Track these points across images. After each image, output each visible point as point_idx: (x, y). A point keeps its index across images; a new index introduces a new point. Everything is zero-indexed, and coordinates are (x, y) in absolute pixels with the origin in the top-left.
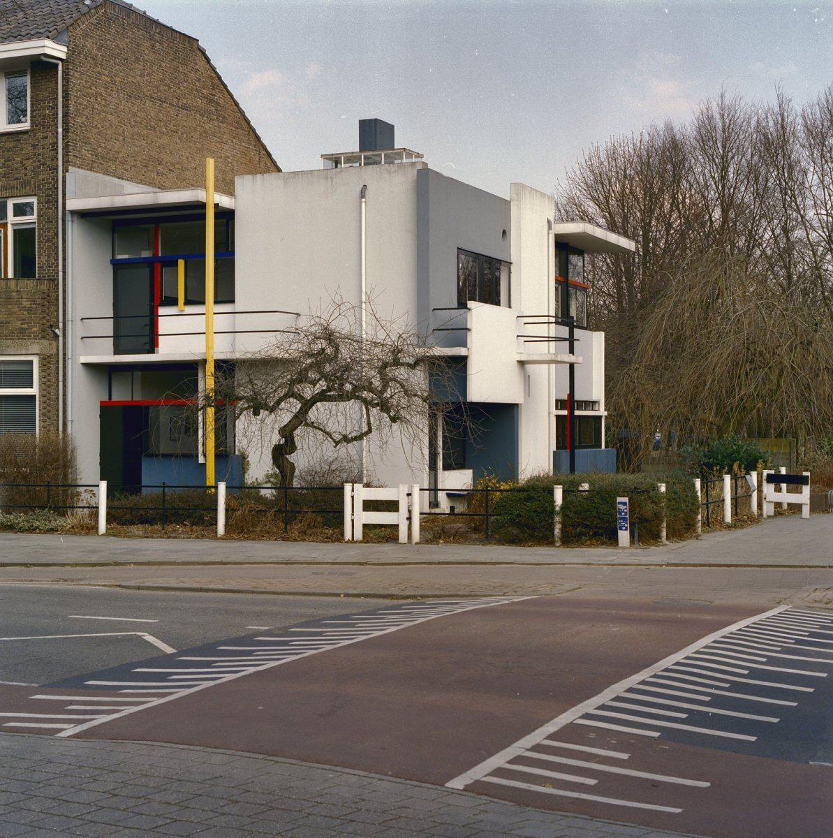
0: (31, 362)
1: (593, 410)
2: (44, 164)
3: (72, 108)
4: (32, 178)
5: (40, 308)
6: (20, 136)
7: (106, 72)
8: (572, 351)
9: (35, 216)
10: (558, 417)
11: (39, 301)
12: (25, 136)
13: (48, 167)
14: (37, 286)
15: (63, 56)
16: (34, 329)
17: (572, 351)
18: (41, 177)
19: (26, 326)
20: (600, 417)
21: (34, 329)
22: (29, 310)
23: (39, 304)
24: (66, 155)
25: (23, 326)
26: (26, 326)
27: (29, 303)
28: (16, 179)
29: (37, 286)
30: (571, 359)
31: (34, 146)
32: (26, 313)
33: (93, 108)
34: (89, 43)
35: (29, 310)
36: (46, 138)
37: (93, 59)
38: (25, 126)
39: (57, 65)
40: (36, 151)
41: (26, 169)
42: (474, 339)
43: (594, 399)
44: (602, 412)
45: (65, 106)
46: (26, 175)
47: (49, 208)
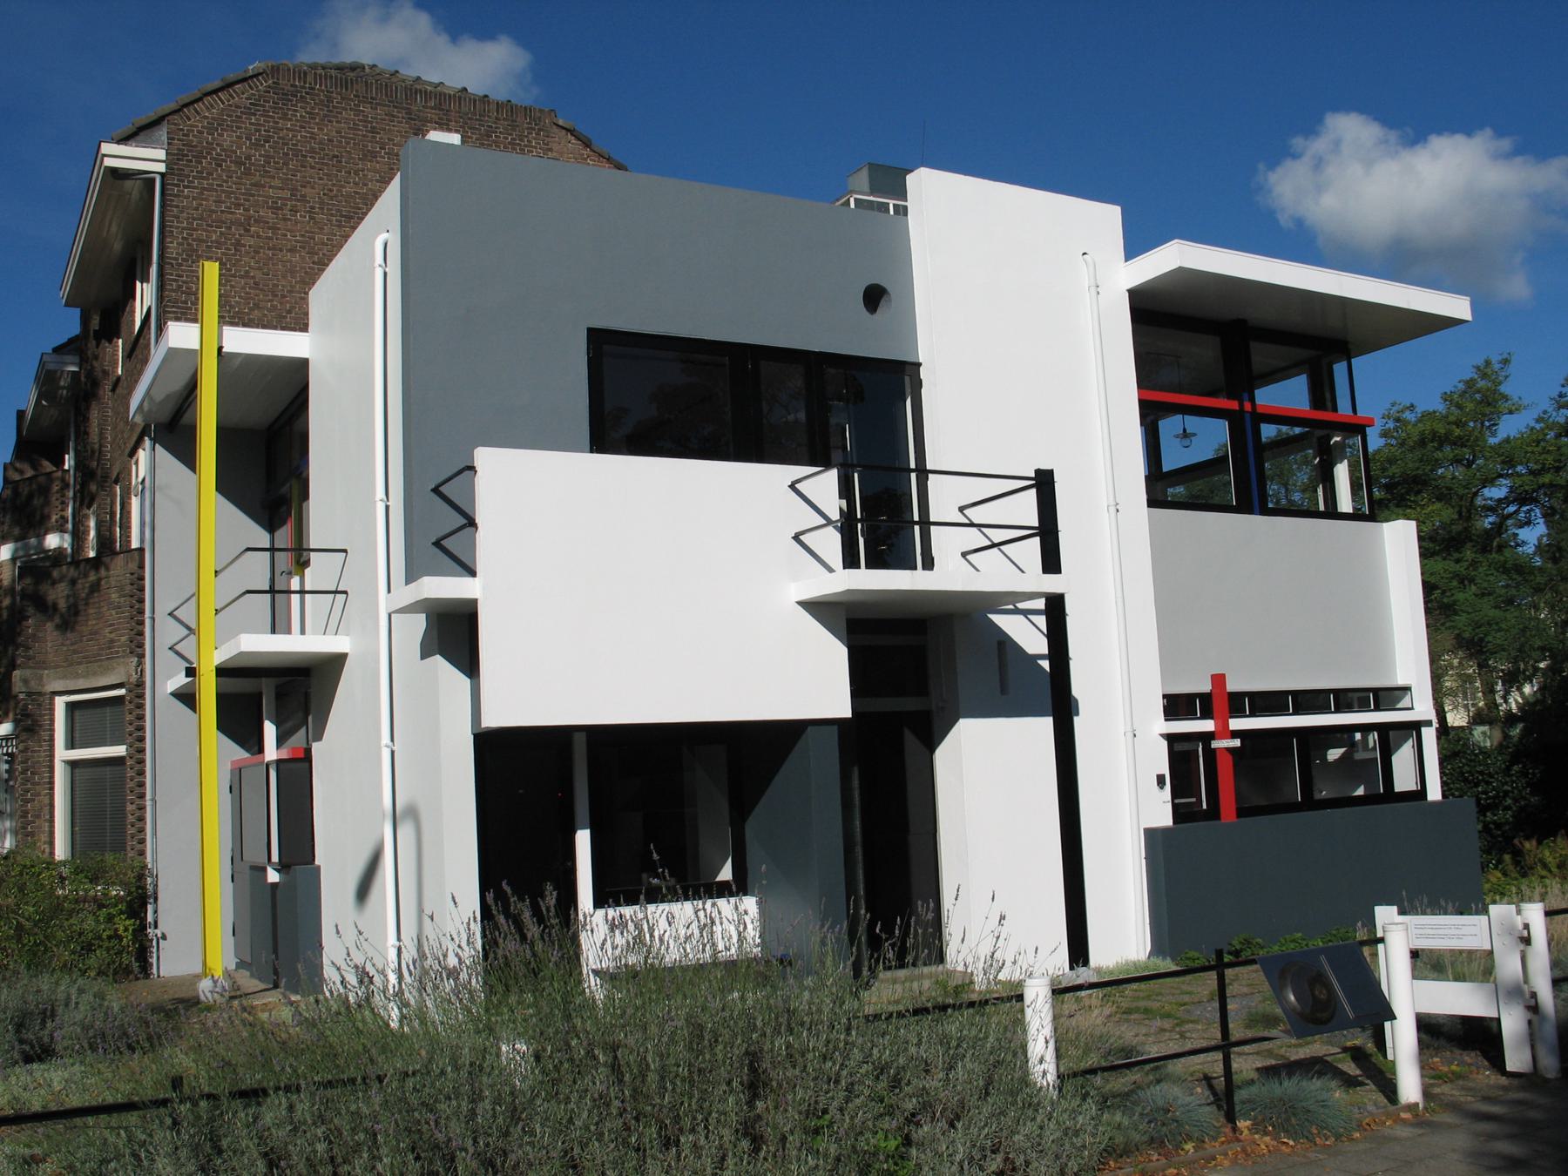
1: (1377, 709)
3: (173, 248)
7: (277, 183)
8: (1051, 563)
10: (1171, 739)
15: (162, 168)
17: (1051, 563)
20: (1415, 727)
30: (1052, 584)
33: (238, 244)
34: (227, 139)
37: (239, 163)
39: (153, 180)
42: (488, 543)
43: (1401, 681)
44: (1421, 707)
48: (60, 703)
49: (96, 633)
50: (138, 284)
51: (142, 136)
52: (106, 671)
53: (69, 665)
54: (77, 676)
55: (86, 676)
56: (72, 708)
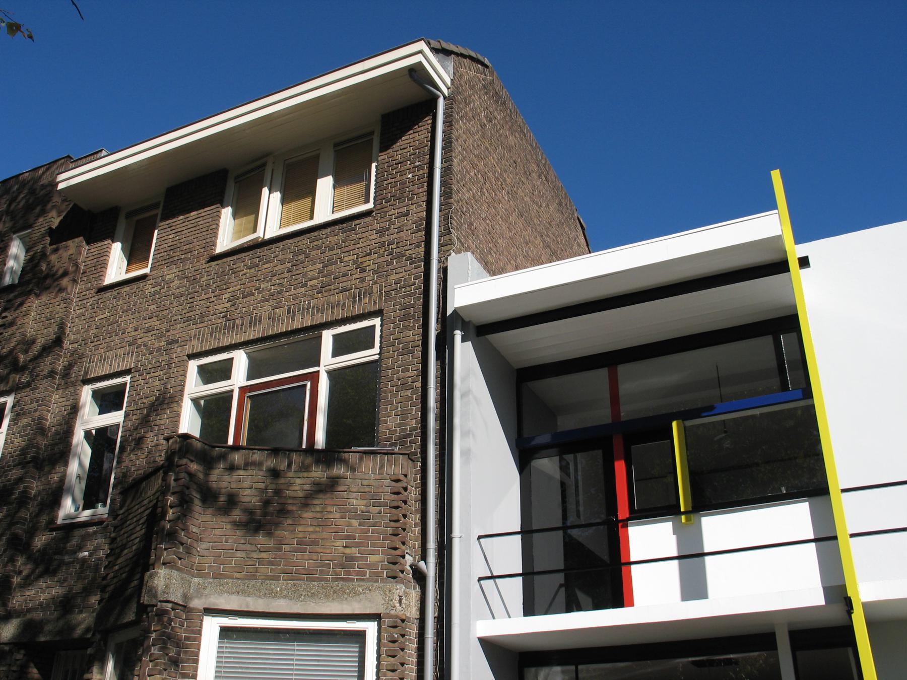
0: (359, 637)
2: (400, 256)
4: (376, 283)
5: (388, 514)
6: (354, 223)
9: (376, 350)
11: (387, 497)
12: (368, 220)
13: (409, 258)
14: (382, 467)
16: (372, 558)
18: (393, 277)
19: (354, 551)
21: (372, 558)
22: (364, 517)
23: (385, 505)
24: (446, 231)
25: (348, 551)
26: (354, 551)
27: (364, 502)
28: (344, 290)
29: (382, 467)
31: (381, 232)
32: (355, 523)
35: (364, 517)
36: (407, 214)
38: (370, 206)
40: (386, 238)
41: (363, 271)
45: (446, 159)
46: (362, 280)
47: (406, 327)
48: (211, 627)
49: (314, 543)
50: (265, 191)
51: (441, 55)
52: (338, 595)
53: (250, 576)
54: (273, 595)
55: (296, 596)
56: (226, 633)
